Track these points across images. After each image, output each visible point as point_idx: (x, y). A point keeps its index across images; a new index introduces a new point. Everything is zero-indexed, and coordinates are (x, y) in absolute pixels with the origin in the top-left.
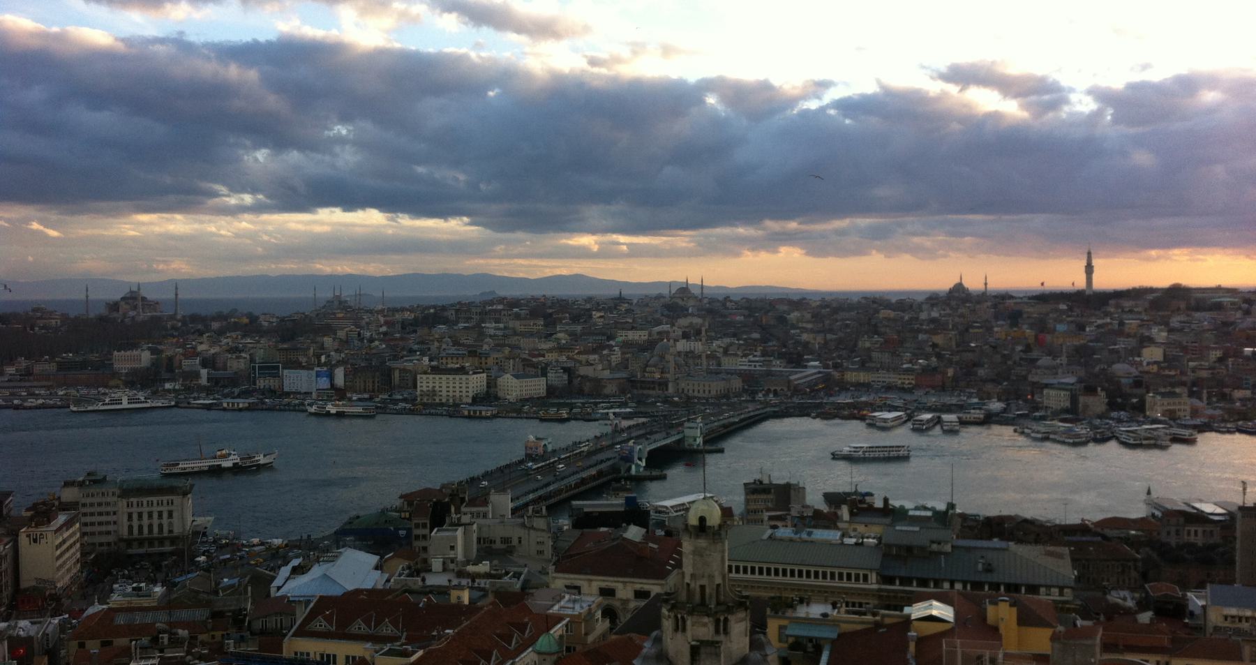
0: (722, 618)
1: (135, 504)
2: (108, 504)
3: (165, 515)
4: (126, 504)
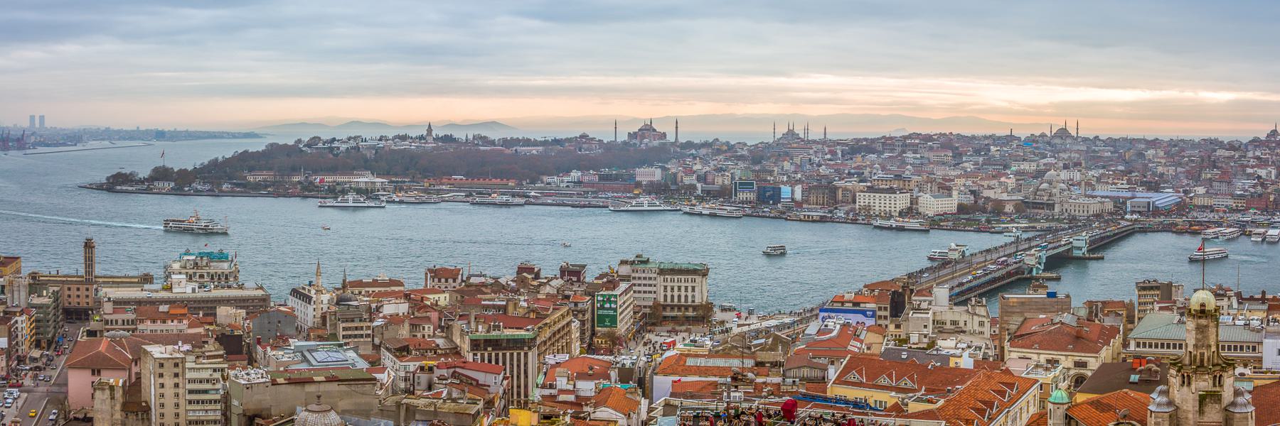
0: (1218, 376)
1: (669, 280)
2: (650, 278)
3: (690, 289)
4: (662, 279)
